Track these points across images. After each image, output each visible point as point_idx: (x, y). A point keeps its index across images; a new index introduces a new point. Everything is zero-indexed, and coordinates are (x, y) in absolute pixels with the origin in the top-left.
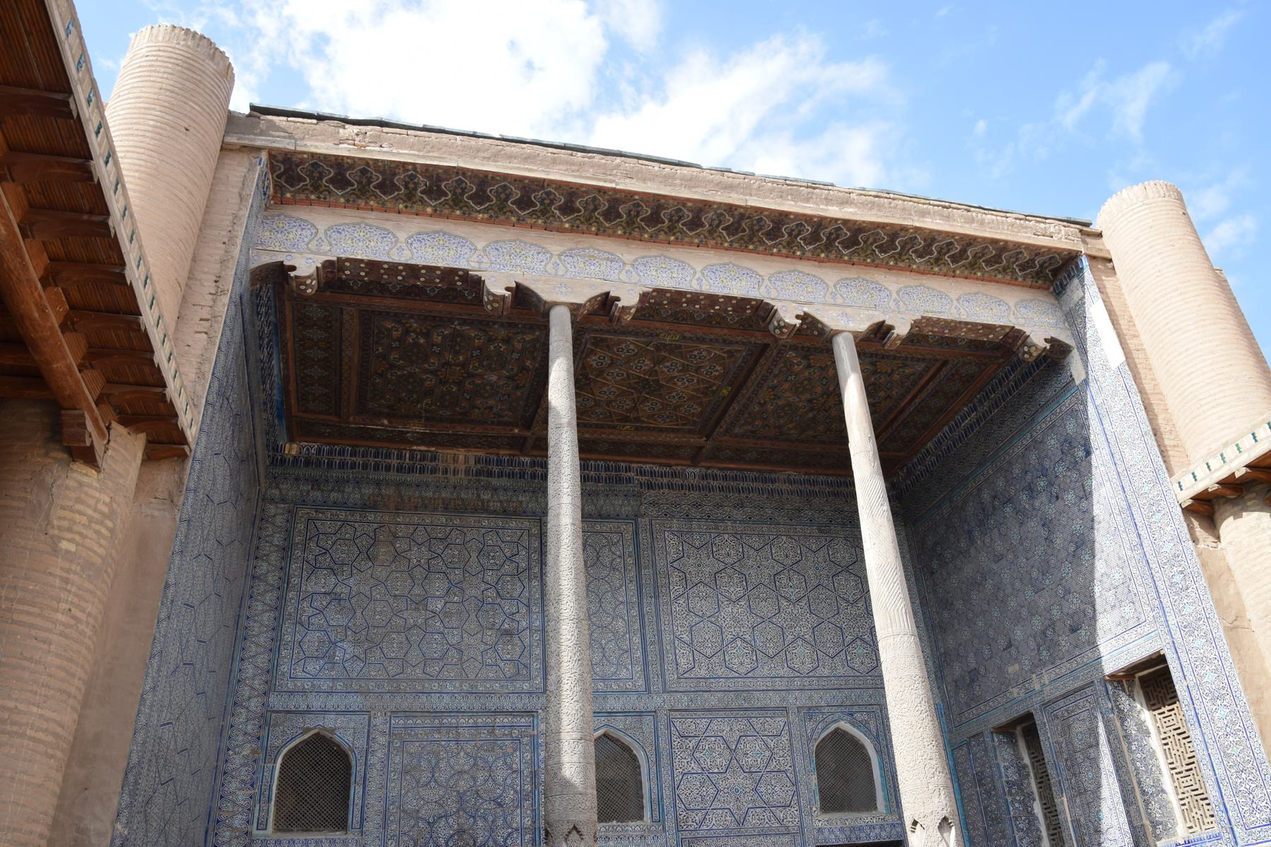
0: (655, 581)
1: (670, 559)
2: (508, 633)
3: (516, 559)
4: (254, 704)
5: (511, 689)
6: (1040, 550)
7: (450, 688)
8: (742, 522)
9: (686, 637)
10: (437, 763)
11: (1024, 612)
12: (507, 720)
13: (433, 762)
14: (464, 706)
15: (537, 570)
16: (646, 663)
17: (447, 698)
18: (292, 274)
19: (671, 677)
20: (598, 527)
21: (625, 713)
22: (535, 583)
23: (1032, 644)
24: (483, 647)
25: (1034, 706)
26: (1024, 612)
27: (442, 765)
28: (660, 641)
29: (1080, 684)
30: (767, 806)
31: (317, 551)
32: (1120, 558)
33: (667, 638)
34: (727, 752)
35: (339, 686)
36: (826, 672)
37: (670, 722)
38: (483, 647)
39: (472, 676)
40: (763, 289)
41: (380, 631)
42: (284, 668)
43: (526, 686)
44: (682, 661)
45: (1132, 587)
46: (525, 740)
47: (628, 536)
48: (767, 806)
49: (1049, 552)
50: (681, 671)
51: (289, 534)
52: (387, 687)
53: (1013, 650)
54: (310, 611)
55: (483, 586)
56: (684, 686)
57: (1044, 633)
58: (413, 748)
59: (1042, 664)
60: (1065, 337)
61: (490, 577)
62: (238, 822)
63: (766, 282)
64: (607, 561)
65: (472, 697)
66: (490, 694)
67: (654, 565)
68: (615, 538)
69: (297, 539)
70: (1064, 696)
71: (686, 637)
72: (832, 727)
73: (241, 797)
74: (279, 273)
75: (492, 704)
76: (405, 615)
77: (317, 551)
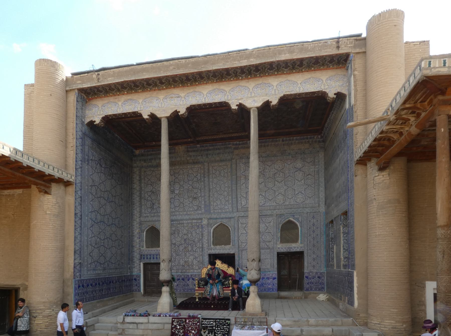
0: (236, 179)
1: (241, 172)
2: (195, 198)
3: (197, 177)
4: (138, 220)
7: (181, 214)
8: (266, 157)
9: (245, 196)
12: (195, 221)
14: (185, 218)
15: (203, 179)
16: (232, 204)
18: (95, 123)
19: (239, 207)
20: (220, 164)
21: (226, 218)
22: (202, 183)
24: (189, 202)
31: (147, 180)
33: (239, 196)
35: (156, 214)
36: (287, 203)
37: (238, 220)
38: (189, 202)
39: (186, 210)
40: (226, 97)
42: (143, 211)
43: (200, 212)
47: (229, 166)
51: (140, 177)
54: (147, 196)
55: (189, 185)
60: (344, 91)
61: (190, 183)
62: (138, 246)
63: (228, 94)
64: (222, 175)
65: (186, 216)
67: (236, 174)
68: (225, 167)
69: (142, 177)
71: (245, 196)
72: (287, 220)
73: (138, 241)
74: (91, 124)
75: (192, 217)
77: (147, 180)
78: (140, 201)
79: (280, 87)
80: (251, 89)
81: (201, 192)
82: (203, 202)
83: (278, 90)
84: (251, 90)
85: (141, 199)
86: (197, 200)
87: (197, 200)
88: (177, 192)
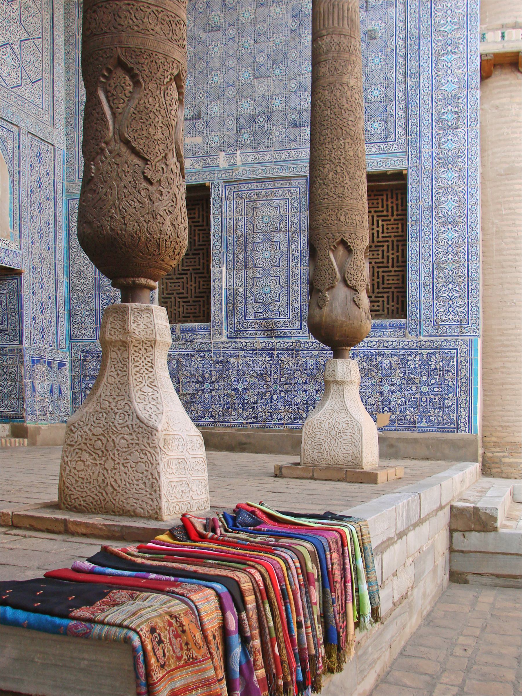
6: (280, 38)
11: (231, 92)
23: (232, 123)
25: (214, 181)
26: (231, 92)
29: (287, 174)
32: (386, 79)
45: (391, 108)
49: (292, 44)
53: (200, 124)
57: (253, 118)
59: (238, 145)
70: (258, 181)
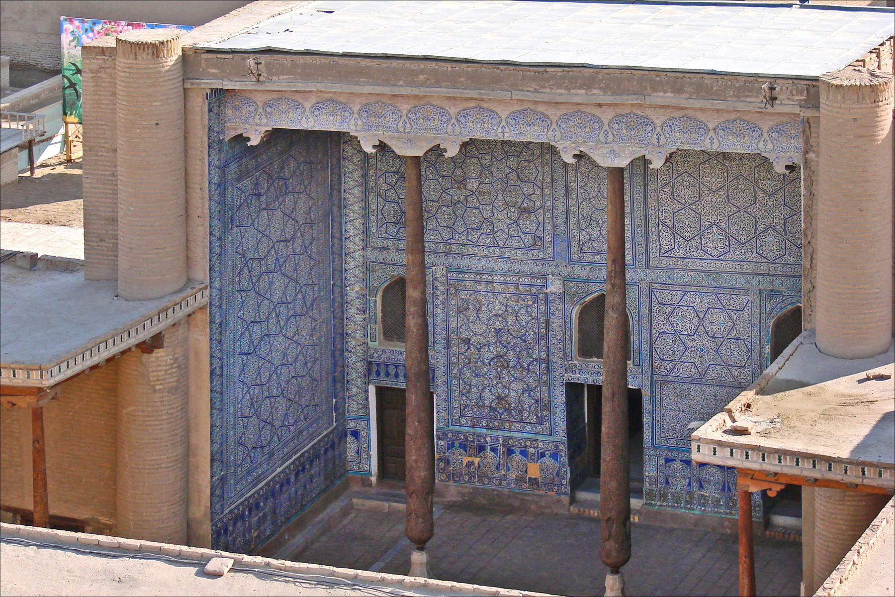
2: (525, 210)
5: (530, 256)
10: (480, 307)
13: (478, 306)
17: (484, 262)
24: (508, 221)
27: (484, 308)
28: (647, 225)
30: (726, 365)
34: (696, 320)
41: (435, 204)
44: (665, 242)
46: (541, 296)
48: (726, 365)
50: (663, 250)
52: (443, 249)
54: (385, 187)
55: (507, 170)
56: (665, 262)
58: (463, 295)
63: (554, 126)
66: (515, 261)
75: (517, 267)
76: (452, 192)
78: (365, 200)
79: (668, 129)
80: (606, 122)
81: (543, 195)
82: (549, 227)
83: (665, 137)
84: (606, 127)
85: (366, 192)
86: (533, 218)
87: (533, 218)
88: (473, 185)
